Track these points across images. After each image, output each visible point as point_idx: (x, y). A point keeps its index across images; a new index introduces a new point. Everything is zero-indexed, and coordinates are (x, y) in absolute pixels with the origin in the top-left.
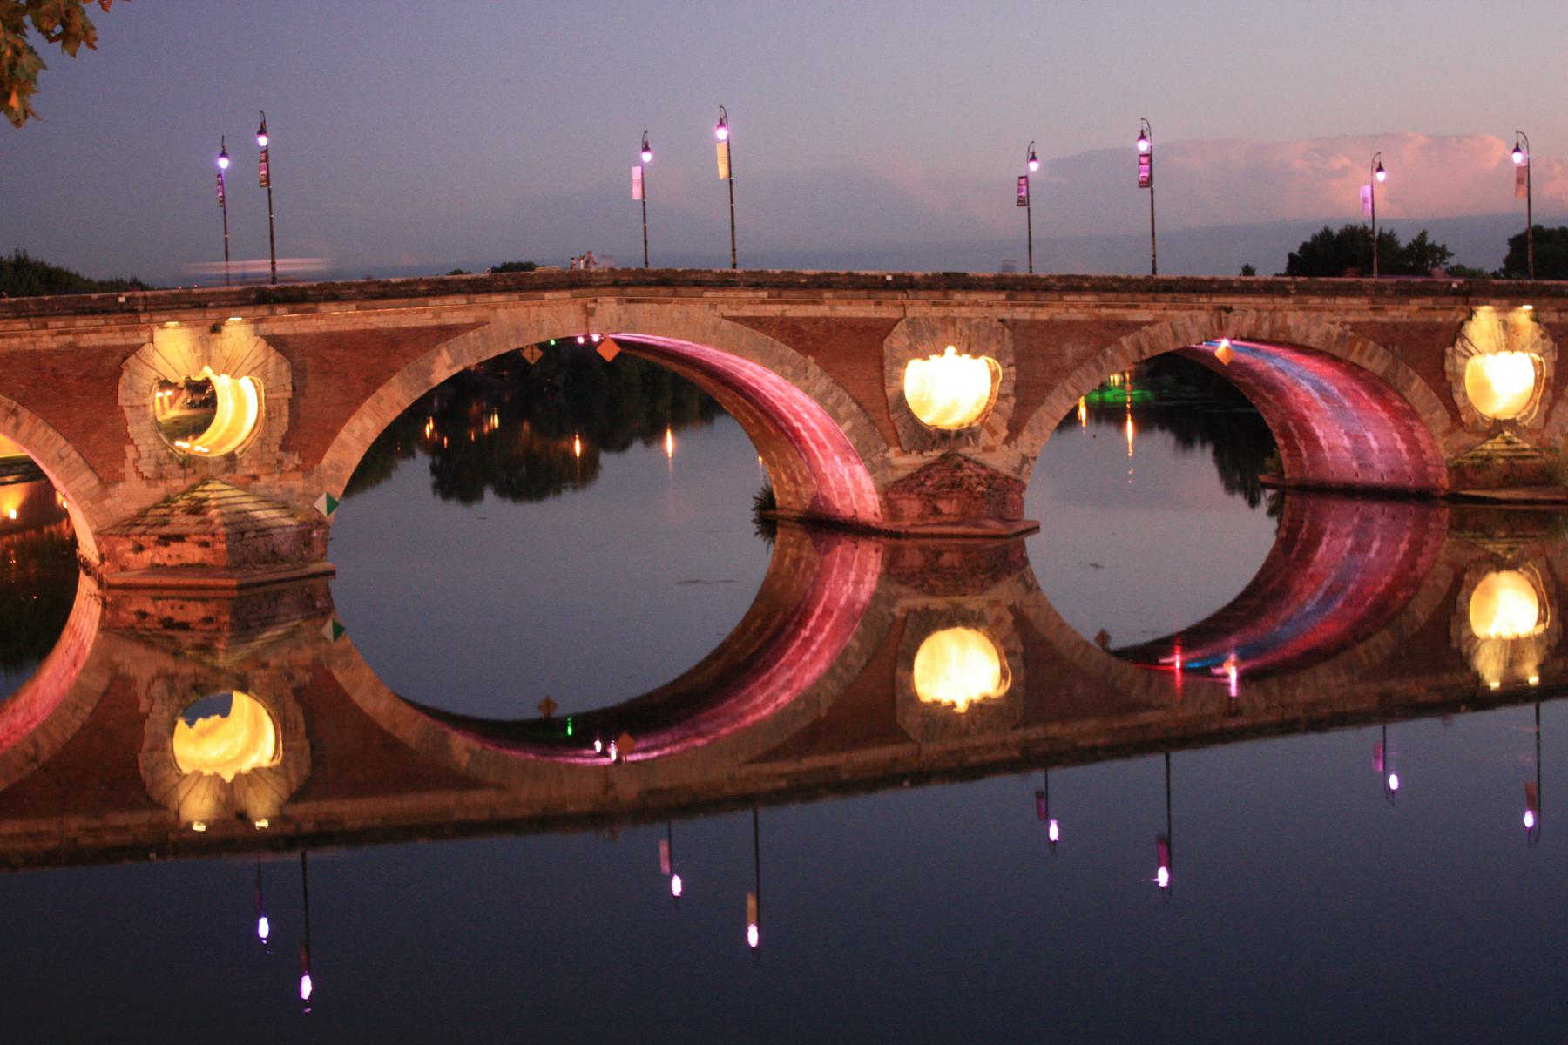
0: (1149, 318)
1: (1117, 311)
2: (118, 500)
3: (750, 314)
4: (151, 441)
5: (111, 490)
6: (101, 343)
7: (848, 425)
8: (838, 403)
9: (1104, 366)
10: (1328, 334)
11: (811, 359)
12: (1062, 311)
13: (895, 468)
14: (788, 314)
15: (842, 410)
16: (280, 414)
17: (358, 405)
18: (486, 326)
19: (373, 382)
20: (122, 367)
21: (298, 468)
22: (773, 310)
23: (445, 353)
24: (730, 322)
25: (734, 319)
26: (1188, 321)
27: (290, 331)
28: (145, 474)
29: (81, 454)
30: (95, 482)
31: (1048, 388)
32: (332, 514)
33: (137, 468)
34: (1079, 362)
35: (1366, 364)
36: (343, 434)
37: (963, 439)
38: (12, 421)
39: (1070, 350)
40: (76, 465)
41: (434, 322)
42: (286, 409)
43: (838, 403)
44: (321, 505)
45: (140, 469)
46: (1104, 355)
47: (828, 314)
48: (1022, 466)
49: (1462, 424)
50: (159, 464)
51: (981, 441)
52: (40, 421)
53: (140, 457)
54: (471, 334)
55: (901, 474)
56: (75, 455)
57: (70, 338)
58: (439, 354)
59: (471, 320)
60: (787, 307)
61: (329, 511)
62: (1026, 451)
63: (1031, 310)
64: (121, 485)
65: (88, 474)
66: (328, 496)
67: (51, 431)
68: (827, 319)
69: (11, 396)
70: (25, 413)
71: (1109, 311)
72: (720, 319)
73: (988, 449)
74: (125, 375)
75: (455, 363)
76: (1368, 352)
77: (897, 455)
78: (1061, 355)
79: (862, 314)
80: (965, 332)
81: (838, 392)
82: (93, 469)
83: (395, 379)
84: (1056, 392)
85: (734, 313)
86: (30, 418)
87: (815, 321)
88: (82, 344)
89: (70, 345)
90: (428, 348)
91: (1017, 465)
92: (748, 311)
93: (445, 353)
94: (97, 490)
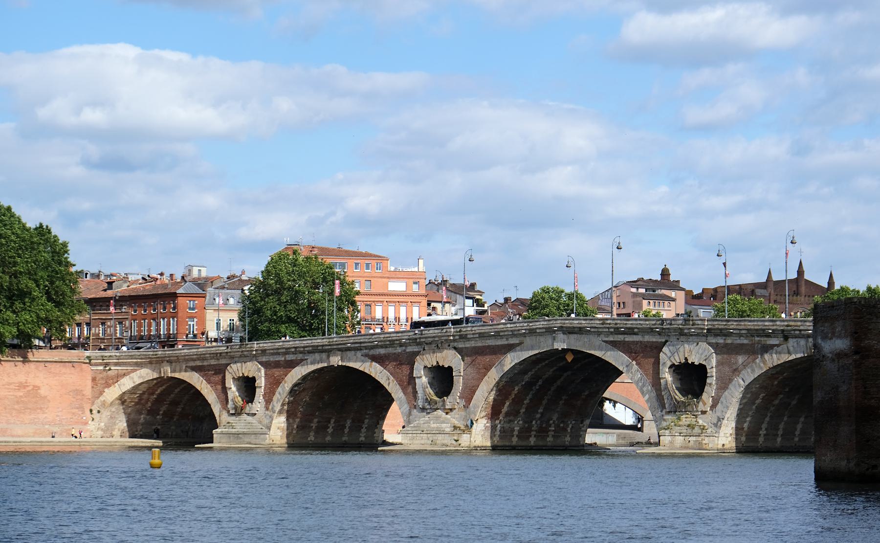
0: (777, 342)
1: (762, 339)
2: (414, 416)
3: (612, 339)
6: (412, 350)
7: (647, 396)
8: (644, 386)
9: (756, 369)
12: (737, 338)
14: (627, 340)
15: (645, 389)
18: (522, 345)
22: (620, 338)
24: (605, 344)
25: (606, 342)
26: (795, 344)
27: (464, 346)
29: (405, 395)
31: (731, 380)
34: (745, 366)
36: (477, 393)
41: (506, 343)
43: (644, 386)
46: (756, 363)
47: (641, 339)
48: (717, 422)
57: (404, 348)
59: (518, 342)
60: (626, 336)
63: (724, 338)
68: (641, 342)
69: (389, 371)
70: (391, 378)
71: (758, 339)
72: (601, 342)
79: (654, 340)
84: (734, 382)
85: (606, 339)
87: (637, 342)
88: (408, 351)
89: (405, 350)
91: (715, 422)
92: (611, 338)
93: (509, 356)
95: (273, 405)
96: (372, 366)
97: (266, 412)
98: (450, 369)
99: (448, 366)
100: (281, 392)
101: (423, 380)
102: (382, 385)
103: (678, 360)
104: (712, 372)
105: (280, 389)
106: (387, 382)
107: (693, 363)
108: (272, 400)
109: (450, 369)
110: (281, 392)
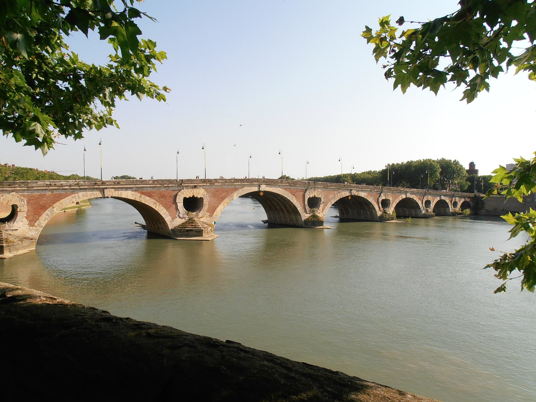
4: (182, 210)
5: (174, 220)
10: (364, 195)
11: (294, 196)
13: (306, 216)
16: (206, 205)
17: (220, 203)
19: (223, 199)
20: (177, 194)
21: (209, 216)
23: (236, 193)
28: (181, 217)
30: (171, 218)
32: (215, 225)
33: (179, 216)
35: (369, 200)
37: (316, 211)
38: (155, 205)
39: (331, 196)
40: (167, 215)
42: (208, 204)
44: (213, 223)
45: (180, 216)
49: (380, 210)
50: (183, 215)
51: (318, 212)
52: (161, 205)
53: (180, 213)
54: (240, 190)
55: (307, 218)
56: (167, 212)
58: (235, 193)
60: (291, 187)
61: (214, 224)
62: (324, 214)
64: (176, 219)
65: (170, 217)
66: (214, 222)
67: (163, 207)
69: (155, 200)
73: (319, 213)
74: (178, 196)
75: (237, 196)
76: (369, 198)
77: (306, 214)
78: (330, 197)
80: (317, 192)
81: (298, 202)
82: (170, 216)
83: (227, 198)
86: (159, 204)
90: (232, 193)
93: (236, 193)
94: (171, 220)
95: (40, 223)
96: (142, 197)
97: (31, 228)
98: (201, 199)
99: (200, 197)
100: (50, 214)
101: (180, 205)
102: (151, 207)
103: (312, 196)
104: (323, 200)
105: (47, 212)
106: (155, 205)
107: (317, 197)
108: (38, 219)
109: (201, 199)
110: (50, 214)
